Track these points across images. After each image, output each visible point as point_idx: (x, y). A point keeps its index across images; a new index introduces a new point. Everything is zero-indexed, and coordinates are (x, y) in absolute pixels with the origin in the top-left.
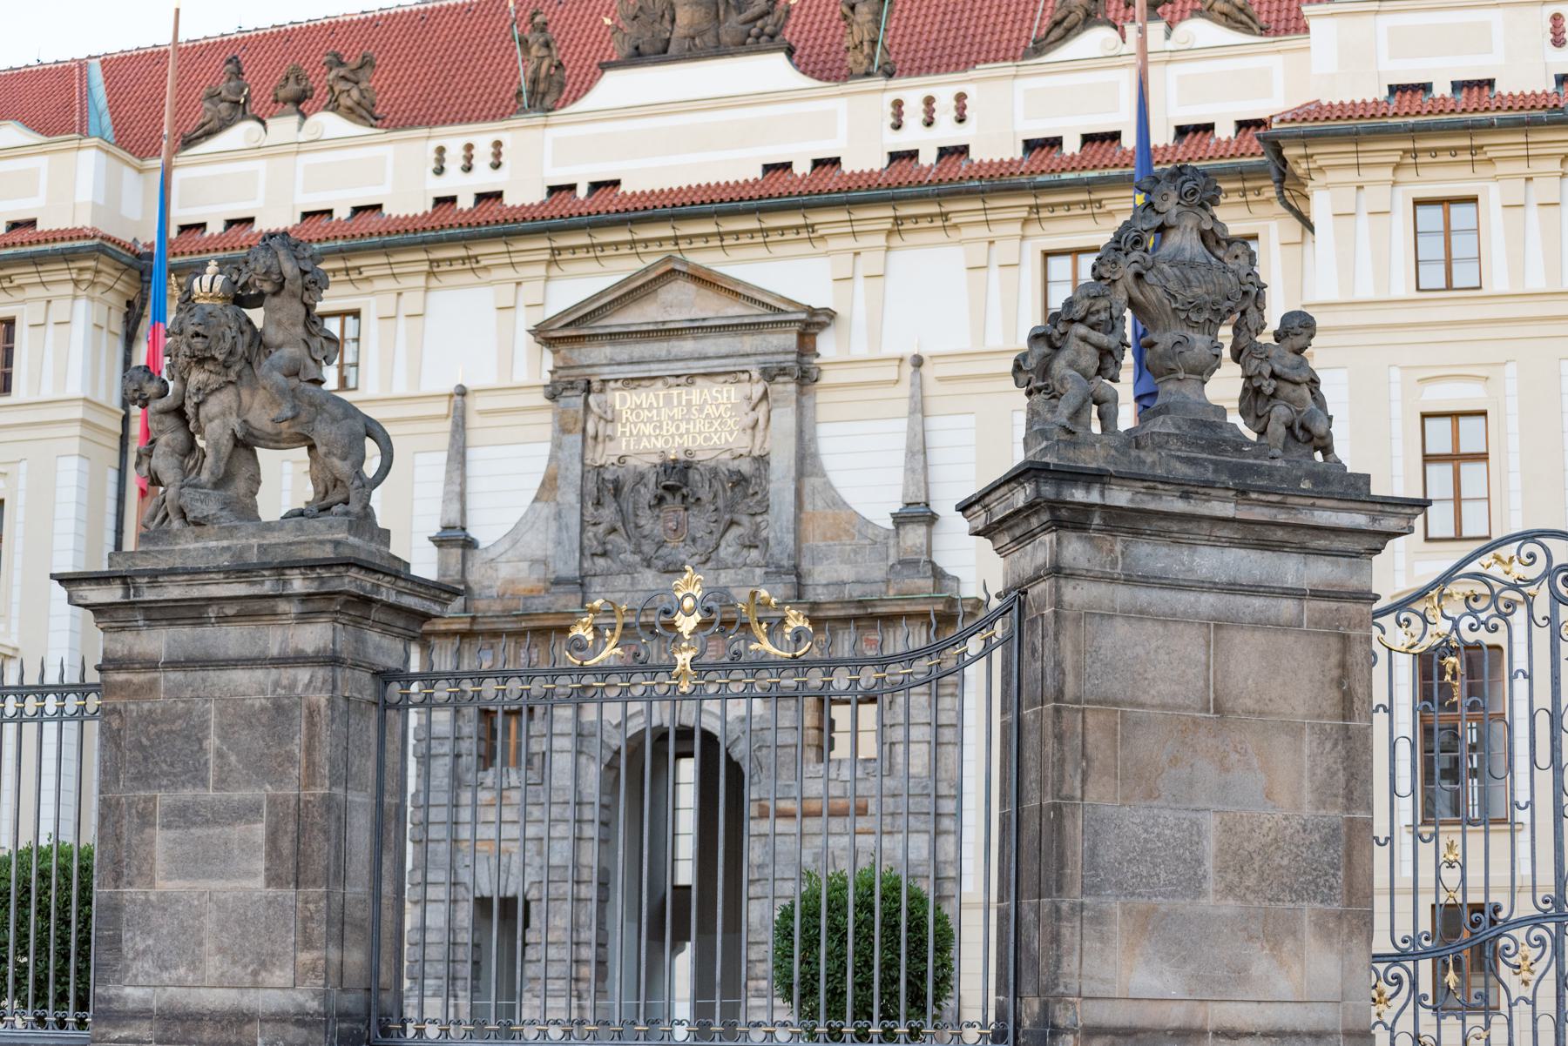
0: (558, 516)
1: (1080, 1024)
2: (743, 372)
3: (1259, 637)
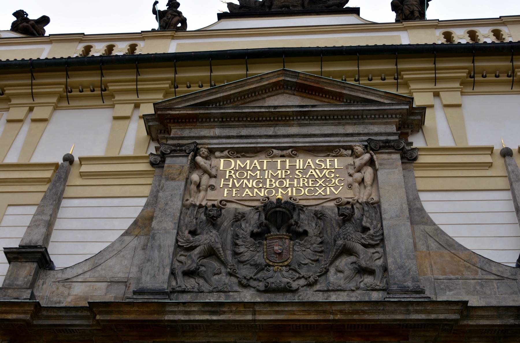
2: (346, 148)
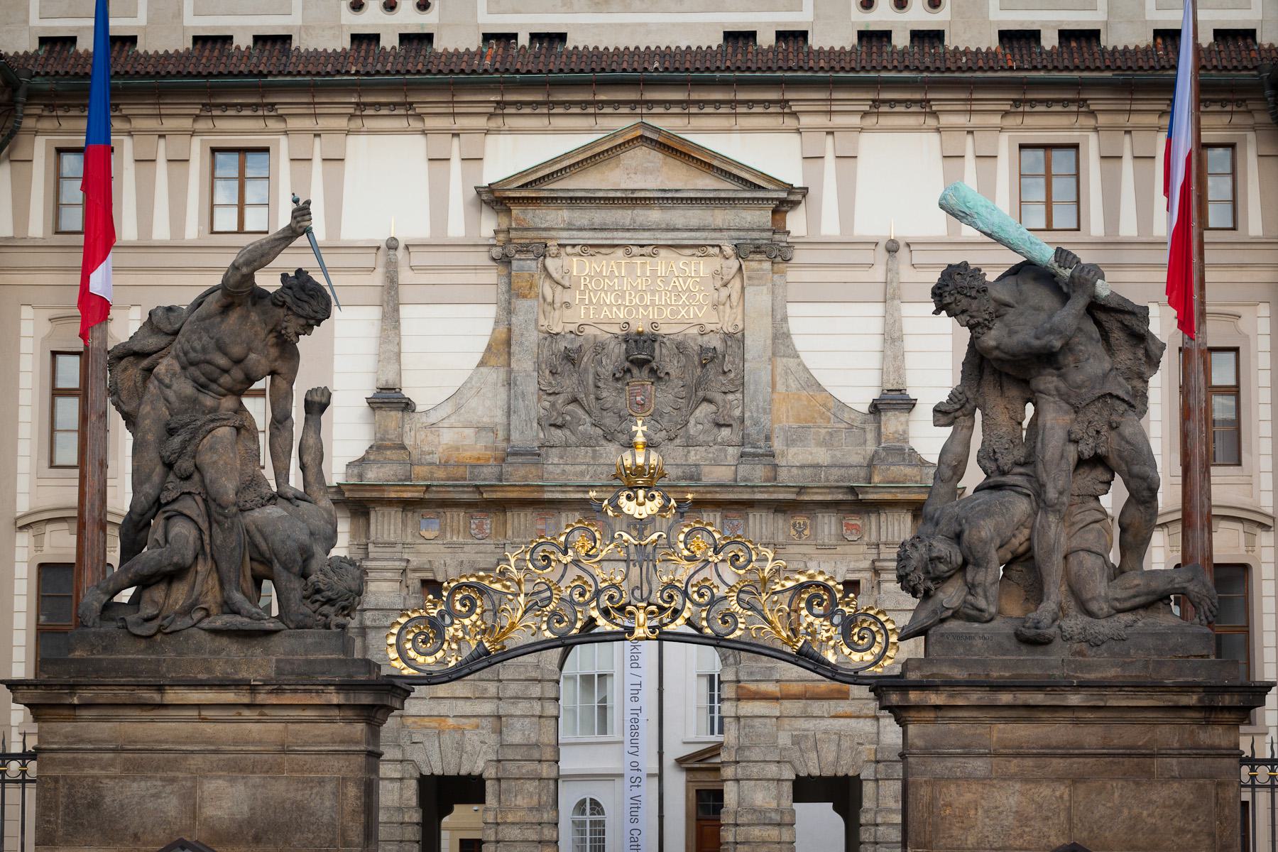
0: (510, 383)
2: (713, 246)
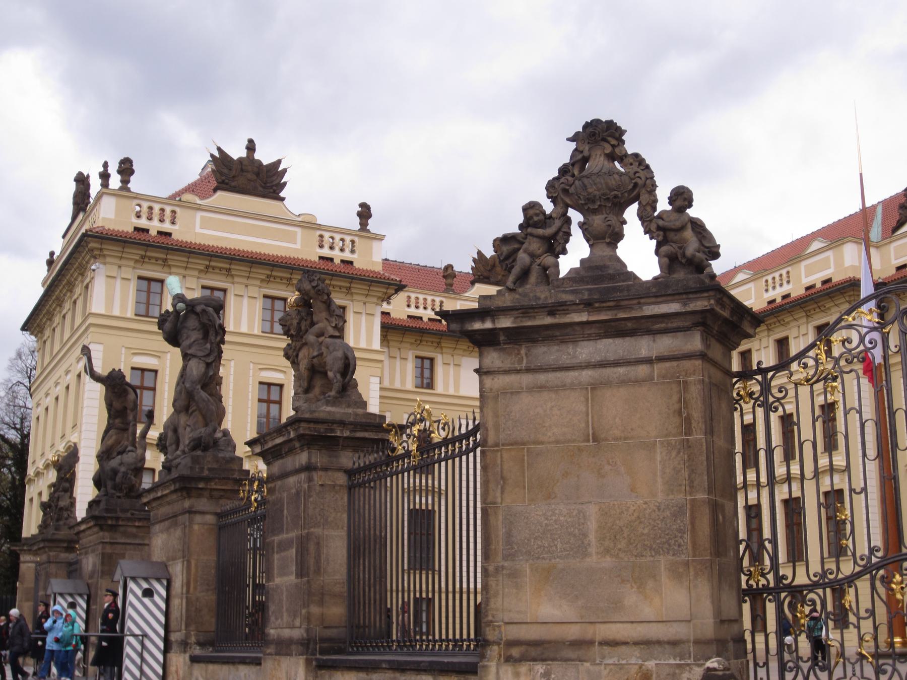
1: (504, 639)
3: (623, 392)
